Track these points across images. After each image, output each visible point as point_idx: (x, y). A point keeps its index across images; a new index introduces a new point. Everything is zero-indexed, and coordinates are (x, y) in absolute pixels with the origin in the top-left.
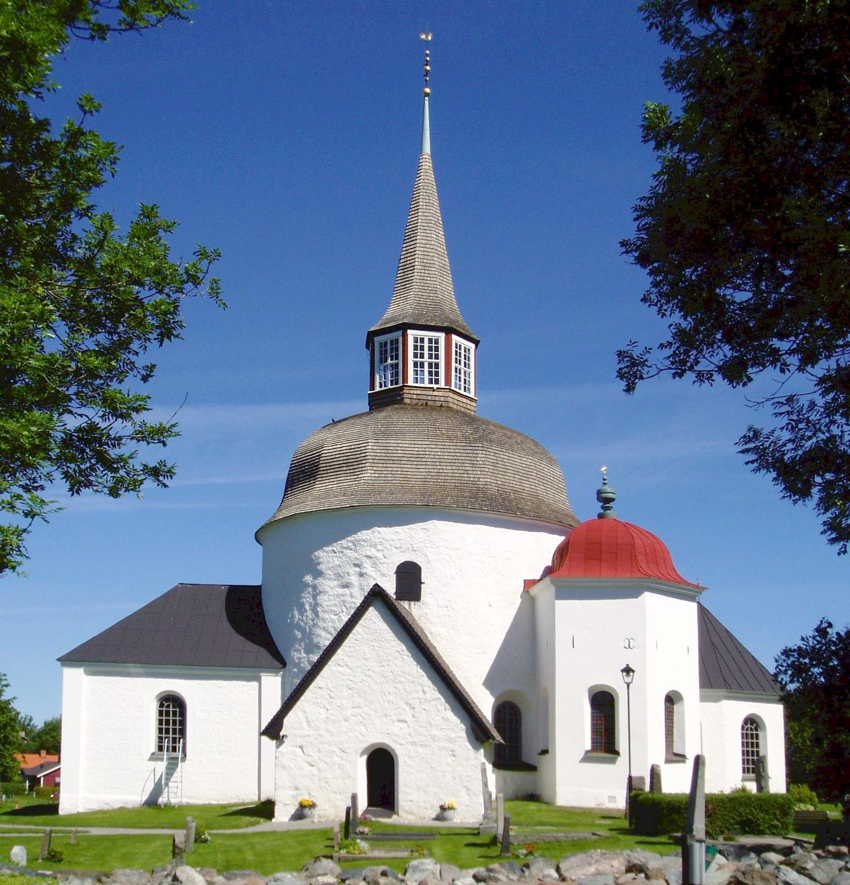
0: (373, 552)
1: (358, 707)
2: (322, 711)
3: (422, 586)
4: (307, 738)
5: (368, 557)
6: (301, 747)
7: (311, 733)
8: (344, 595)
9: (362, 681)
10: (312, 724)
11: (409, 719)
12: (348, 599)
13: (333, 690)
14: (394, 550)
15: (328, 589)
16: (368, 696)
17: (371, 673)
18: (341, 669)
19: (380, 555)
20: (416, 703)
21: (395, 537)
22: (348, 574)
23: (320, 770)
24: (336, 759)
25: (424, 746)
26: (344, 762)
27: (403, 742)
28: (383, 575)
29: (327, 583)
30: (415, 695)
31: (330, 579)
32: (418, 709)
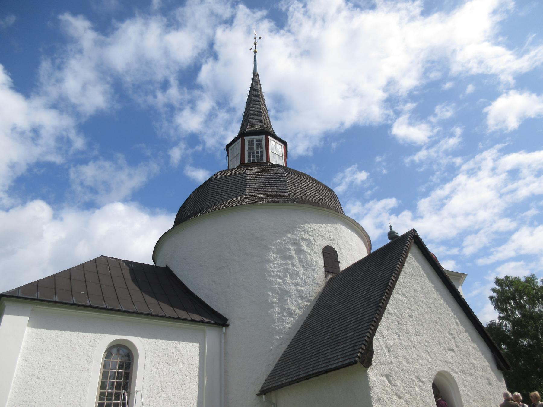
0: (306, 236)
1: (420, 335)
2: (396, 337)
3: (340, 264)
4: (390, 366)
5: (304, 239)
6: (387, 376)
7: (393, 360)
8: (286, 264)
9: (417, 310)
10: (392, 350)
11: (455, 348)
12: (291, 267)
13: (399, 316)
14: (320, 238)
15: (272, 259)
16: (424, 324)
17: (421, 303)
18: (400, 297)
19: (311, 238)
20: (456, 335)
21: (320, 229)
22: (289, 249)
23: (407, 402)
24: (417, 389)
25: (471, 375)
26: (424, 393)
27: (457, 370)
28: (315, 253)
29: (271, 254)
30: (453, 327)
31: (273, 252)
32: (457, 338)
